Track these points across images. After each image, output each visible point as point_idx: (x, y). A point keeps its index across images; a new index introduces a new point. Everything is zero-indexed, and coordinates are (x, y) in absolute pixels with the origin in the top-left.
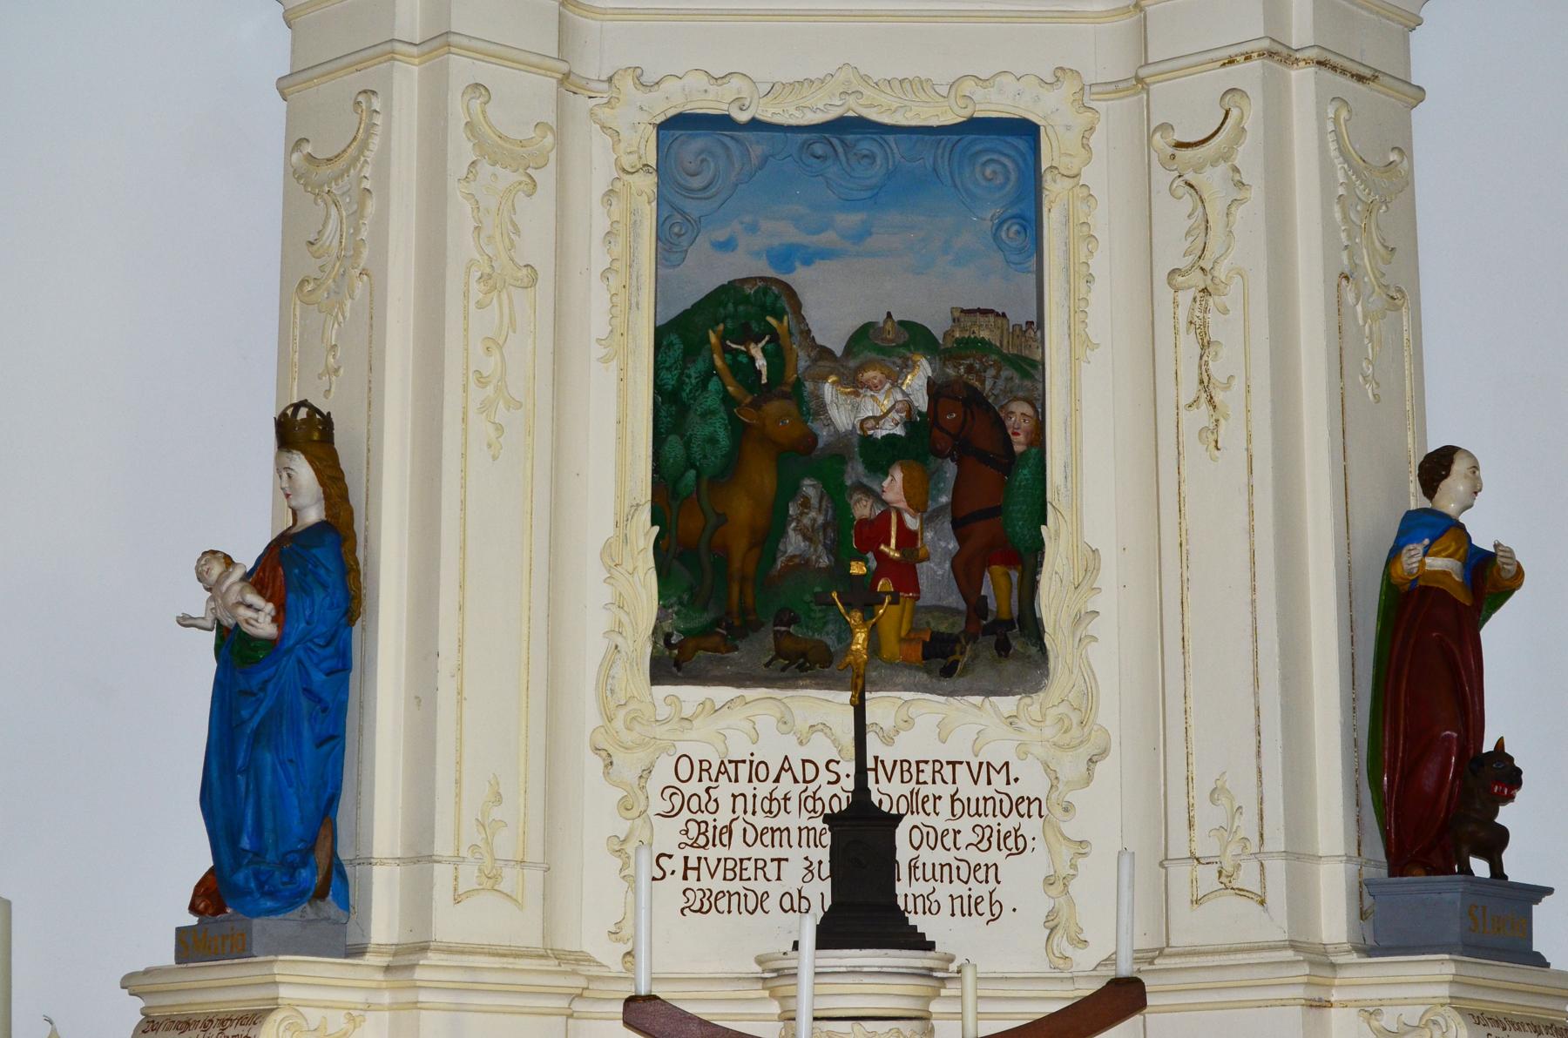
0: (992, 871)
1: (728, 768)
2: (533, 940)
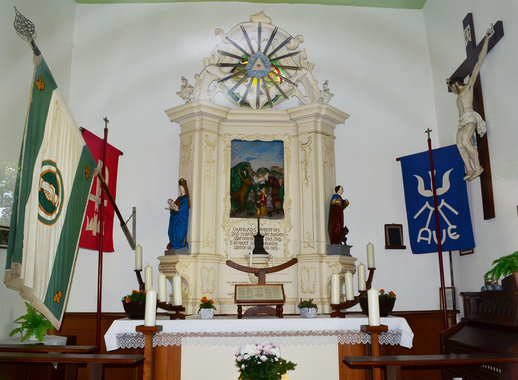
1: (240, 229)
2: (214, 253)
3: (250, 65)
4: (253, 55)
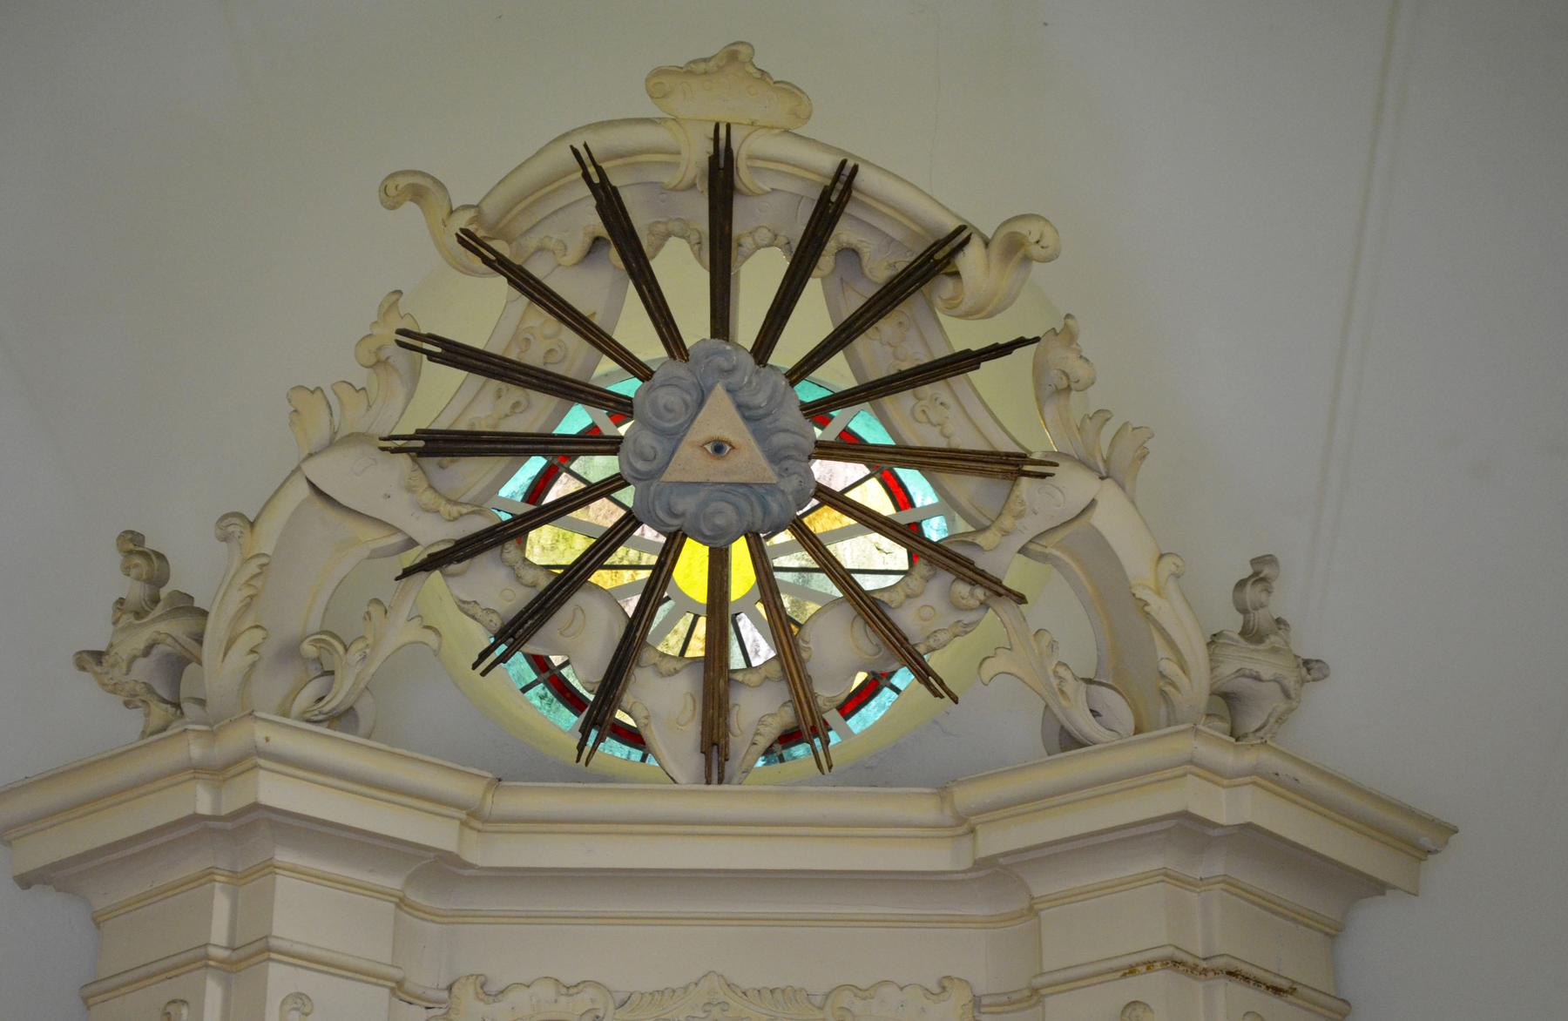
3: (648, 440)
4: (679, 369)
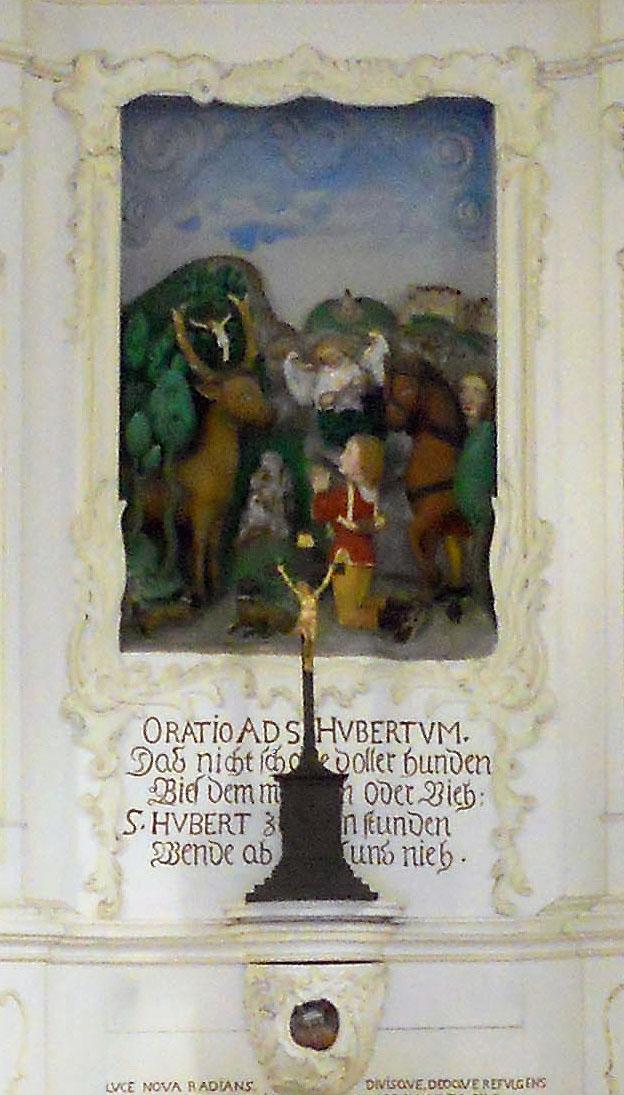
0: (443, 824)
1: (193, 728)
